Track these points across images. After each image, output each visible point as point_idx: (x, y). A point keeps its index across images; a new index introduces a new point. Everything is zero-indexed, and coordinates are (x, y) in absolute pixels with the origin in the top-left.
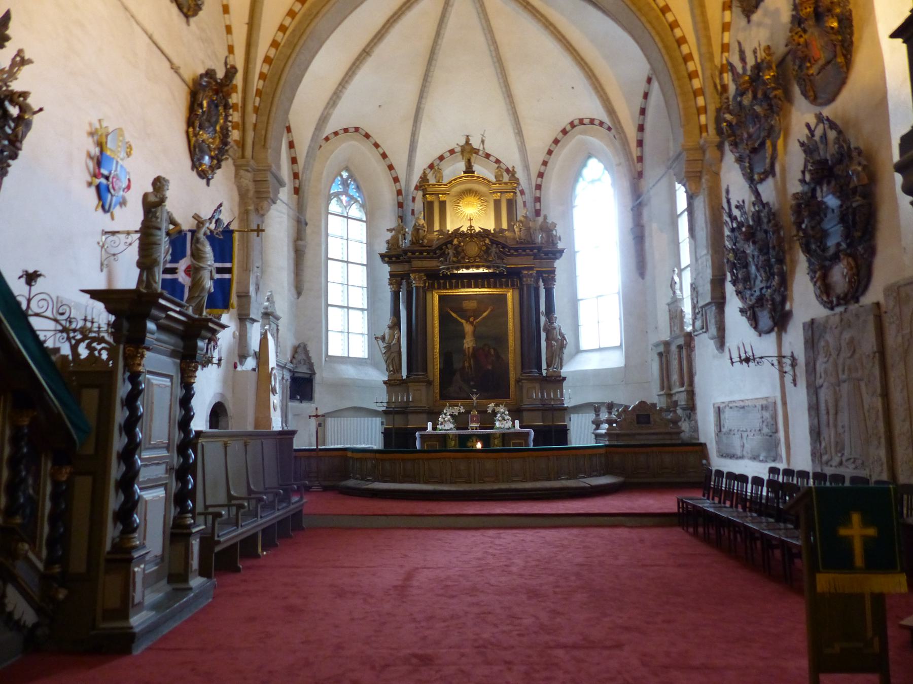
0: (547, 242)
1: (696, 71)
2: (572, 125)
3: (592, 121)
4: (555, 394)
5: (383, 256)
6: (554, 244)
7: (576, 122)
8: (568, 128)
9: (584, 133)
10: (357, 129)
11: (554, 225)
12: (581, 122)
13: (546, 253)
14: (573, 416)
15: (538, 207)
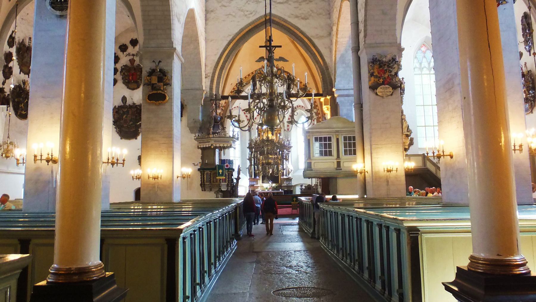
0: (289, 144)
1: (320, 113)
2: (297, 106)
3: (303, 107)
4: (290, 183)
5: (247, 148)
6: (290, 145)
7: (298, 106)
8: (297, 107)
9: (300, 109)
10: (238, 107)
11: (290, 140)
12: (300, 106)
13: (288, 147)
14: (297, 187)
15: (288, 128)
